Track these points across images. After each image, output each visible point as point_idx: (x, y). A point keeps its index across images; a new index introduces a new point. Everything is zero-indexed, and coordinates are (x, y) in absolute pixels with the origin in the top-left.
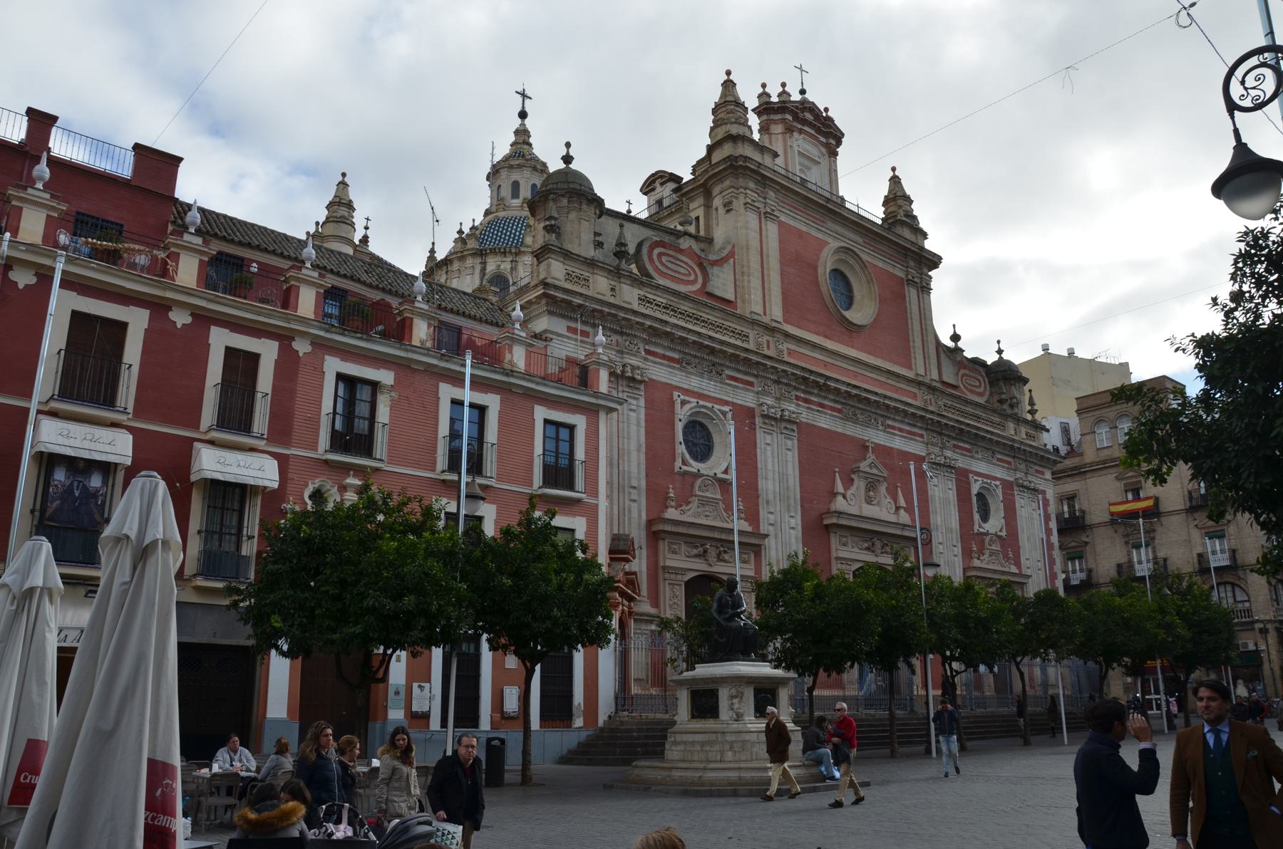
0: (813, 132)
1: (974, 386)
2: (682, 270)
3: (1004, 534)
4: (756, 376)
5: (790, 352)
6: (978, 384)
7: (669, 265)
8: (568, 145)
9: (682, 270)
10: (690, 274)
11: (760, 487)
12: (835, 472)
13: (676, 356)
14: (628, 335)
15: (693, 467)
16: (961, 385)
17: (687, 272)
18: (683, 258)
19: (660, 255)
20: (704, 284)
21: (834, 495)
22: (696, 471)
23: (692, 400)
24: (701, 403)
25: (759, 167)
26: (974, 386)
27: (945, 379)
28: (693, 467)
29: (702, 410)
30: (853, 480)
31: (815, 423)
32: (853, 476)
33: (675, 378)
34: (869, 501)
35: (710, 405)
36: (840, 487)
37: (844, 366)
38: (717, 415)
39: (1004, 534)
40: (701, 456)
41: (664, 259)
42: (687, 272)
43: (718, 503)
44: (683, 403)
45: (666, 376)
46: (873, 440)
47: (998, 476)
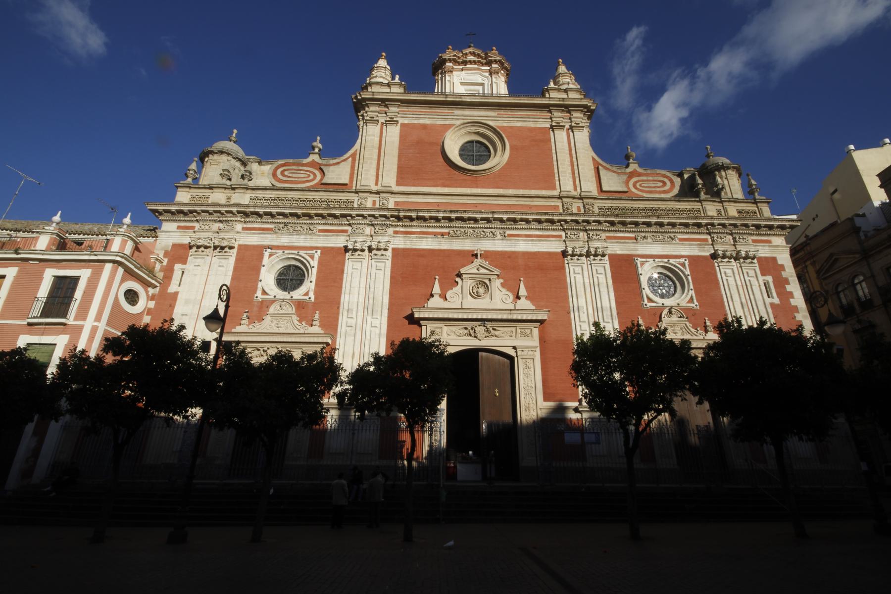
0: (476, 66)
1: (659, 187)
2: (302, 176)
3: (695, 304)
4: (350, 225)
5: (397, 203)
6: (661, 184)
7: (291, 175)
9: (302, 176)
10: (309, 176)
12: (435, 279)
15: (270, 295)
16: (634, 190)
17: (307, 176)
18: (305, 168)
19: (282, 173)
20: (321, 179)
21: (432, 296)
22: (272, 297)
23: (277, 251)
24: (286, 252)
25: (373, 95)
26: (659, 187)
27: (604, 189)
30: (457, 283)
31: (414, 247)
32: (458, 279)
33: (268, 240)
34: (476, 296)
35: (296, 252)
36: (437, 289)
37: (461, 201)
39: (695, 304)
40: (291, 287)
41: (286, 173)
42: (307, 176)
44: (270, 256)
45: (260, 240)
46: (481, 249)
47: (684, 253)
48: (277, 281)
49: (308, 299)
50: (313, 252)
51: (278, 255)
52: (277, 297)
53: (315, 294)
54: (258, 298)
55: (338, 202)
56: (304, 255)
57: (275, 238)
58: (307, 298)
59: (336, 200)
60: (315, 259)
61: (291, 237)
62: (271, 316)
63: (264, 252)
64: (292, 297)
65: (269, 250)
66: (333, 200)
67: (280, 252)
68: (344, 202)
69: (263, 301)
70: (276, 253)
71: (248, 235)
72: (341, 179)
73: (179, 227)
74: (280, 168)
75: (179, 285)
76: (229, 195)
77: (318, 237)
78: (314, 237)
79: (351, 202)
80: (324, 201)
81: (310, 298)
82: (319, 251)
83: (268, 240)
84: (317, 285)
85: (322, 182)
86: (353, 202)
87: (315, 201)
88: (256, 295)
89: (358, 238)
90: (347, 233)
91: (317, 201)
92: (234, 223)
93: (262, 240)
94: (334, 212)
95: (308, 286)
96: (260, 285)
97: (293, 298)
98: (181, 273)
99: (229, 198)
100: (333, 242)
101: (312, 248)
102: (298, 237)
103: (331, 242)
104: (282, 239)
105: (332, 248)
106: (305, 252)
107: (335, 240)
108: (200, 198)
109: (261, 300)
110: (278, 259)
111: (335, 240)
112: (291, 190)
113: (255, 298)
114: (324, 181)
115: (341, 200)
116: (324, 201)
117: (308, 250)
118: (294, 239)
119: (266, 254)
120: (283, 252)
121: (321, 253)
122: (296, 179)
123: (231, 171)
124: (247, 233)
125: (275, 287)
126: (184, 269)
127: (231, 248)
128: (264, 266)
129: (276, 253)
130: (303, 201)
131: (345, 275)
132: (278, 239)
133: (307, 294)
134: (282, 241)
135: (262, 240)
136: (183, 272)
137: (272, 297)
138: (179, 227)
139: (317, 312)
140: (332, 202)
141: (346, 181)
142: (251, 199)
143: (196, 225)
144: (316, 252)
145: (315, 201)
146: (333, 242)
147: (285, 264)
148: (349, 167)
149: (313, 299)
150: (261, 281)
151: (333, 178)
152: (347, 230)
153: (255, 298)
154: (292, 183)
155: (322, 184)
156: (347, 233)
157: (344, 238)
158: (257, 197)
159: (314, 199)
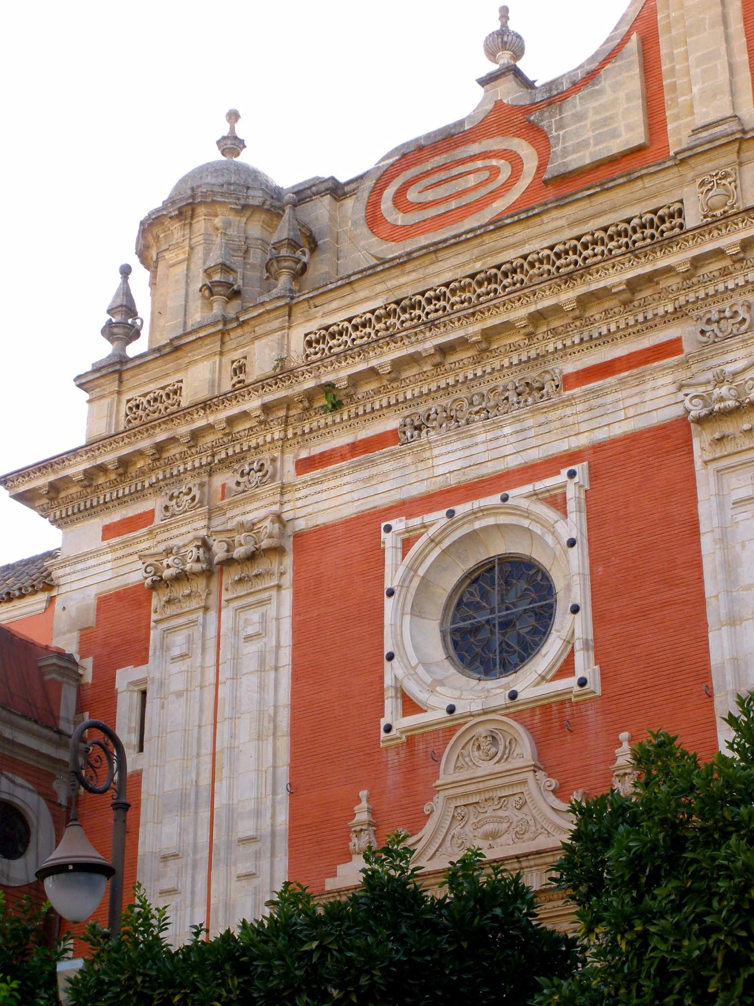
2: (472, 181)
4: (680, 313)
7: (430, 196)
8: (233, 116)
9: (472, 181)
10: (495, 172)
11: (715, 657)
13: (391, 423)
14: (241, 457)
15: (434, 709)
18: (474, 149)
20: (541, 167)
23: (428, 518)
24: (461, 509)
28: (434, 709)
29: (477, 525)
33: (387, 486)
35: (494, 500)
38: (527, 514)
41: (412, 195)
42: (485, 175)
43: (525, 782)
48: (455, 644)
49: (577, 688)
50: (562, 477)
51: (431, 531)
52: (458, 712)
53: (601, 655)
54: (393, 732)
55: (619, 234)
56: (524, 504)
57: (412, 468)
58: (570, 683)
59: (612, 230)
60: (571, 506)
61: (467, 442)
62: (449, 798)
63: (383, 535)
64: (513, 696)
65: (399, 524)
66: (599, 234)
67: (438, 517)
68: (643, 226)
69: (411, 741)
70: (425, 526)
71: (318, 488)
72: (614, 134)
73: (109, 531)
74: (382, 190)
75: (141, 749)
76: (237, 355)
77: (568, 411)
78: (552, 415)
79: (671, 216)
80: (566, 252)
81: (582, 682)
82: (581, 468)
83: (387, 486)
84: (599, 619)
85: (546, 176)
86: (680, 213)
87: (531, 264)
88: (383, 722)
89: (730, 357)
90: (680, 351)
91: (541, 262)
92: (266, 456)
93: (371, 491)
94: (602, 284)
95: (564, 634)
96: (392, 672)
97: (521, 697)
98: (136, 698)
99: (240, 368)
100: (631, 412)
101: (551, 465)
102: (490, 435)
103: (622, 415)
104: (436, 461)
105: (632, 439)
106: (528, 488)
107: (636, 400)
108: (155, 400)
109: (404, 739)
110: (437, 552)
111: (636, 400)
112: (435, 250)
113: (383, 735)
114: (552, 170)
115: (628, 221)
116: (566, 252)
117: (539, 479)
118: (481, 448)
119: (389, 541)
120: (451, 514)
121: (594, 475)
122: (453, 205)
123: (236, 261)
124: (315, 482)
125: (452, 670)
126: (144, 681)
127: (278, 551)
128: (391, 593)
129: (425, 526)
130: (489, 280)
131: (707, 544)
132: (421, 466)
133: (566, 668)
134: (439, 471)
135: (371, 491)
136: (144, 693)
137: (443, 714)
138: (109, 531)
139: (624, 736)
140: (595, 242)
141: (637, 136)
142: (309, 344)
143: (154, 503)
144: (572, 474)
145: (531, 264)
146: (631, 412)
147: (471, 564)
148: (636, 71)
149: (595, 685)
150: (391, 657)
151: (583, 145)
152: (678, 340)
153: (383, 735)
154: (441, 226)
155: (546, 182)
156: (680, 351)
157: (670, 379)
158: (326, 328)
159: (525, 257)
